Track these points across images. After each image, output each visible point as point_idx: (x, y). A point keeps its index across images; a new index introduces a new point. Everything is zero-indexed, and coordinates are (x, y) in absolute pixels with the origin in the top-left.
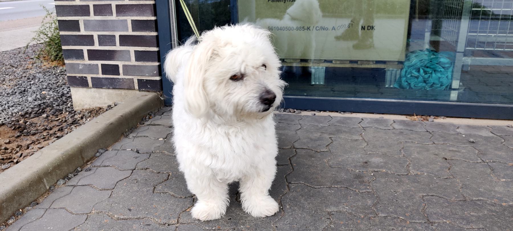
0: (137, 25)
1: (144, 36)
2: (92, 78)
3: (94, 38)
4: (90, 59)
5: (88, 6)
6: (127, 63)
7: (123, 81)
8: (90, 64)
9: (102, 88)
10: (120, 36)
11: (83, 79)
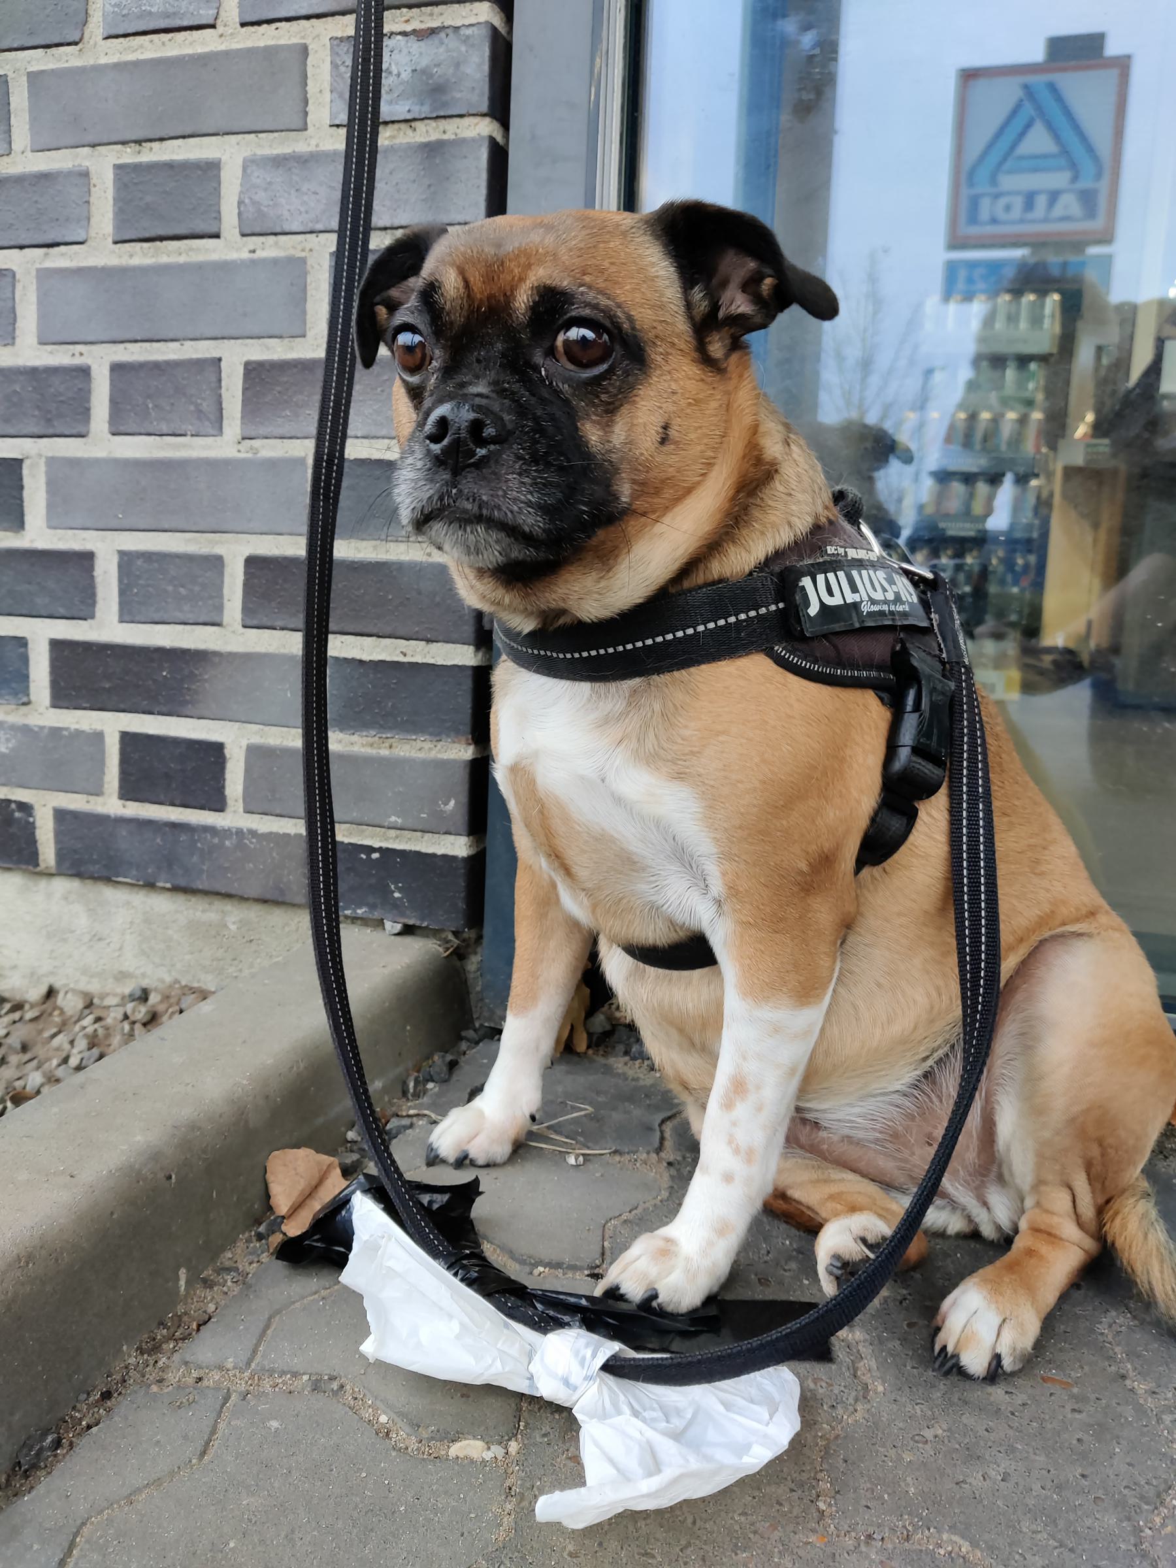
1: (400, 566)
2: (61, 815)
3: (98, 572)
4: (62, 697)
5: (84, 372)
7: (240, 846)
8: (56, 732)
9: (108, 880)
10: (252, 563)
11: (9, 821)
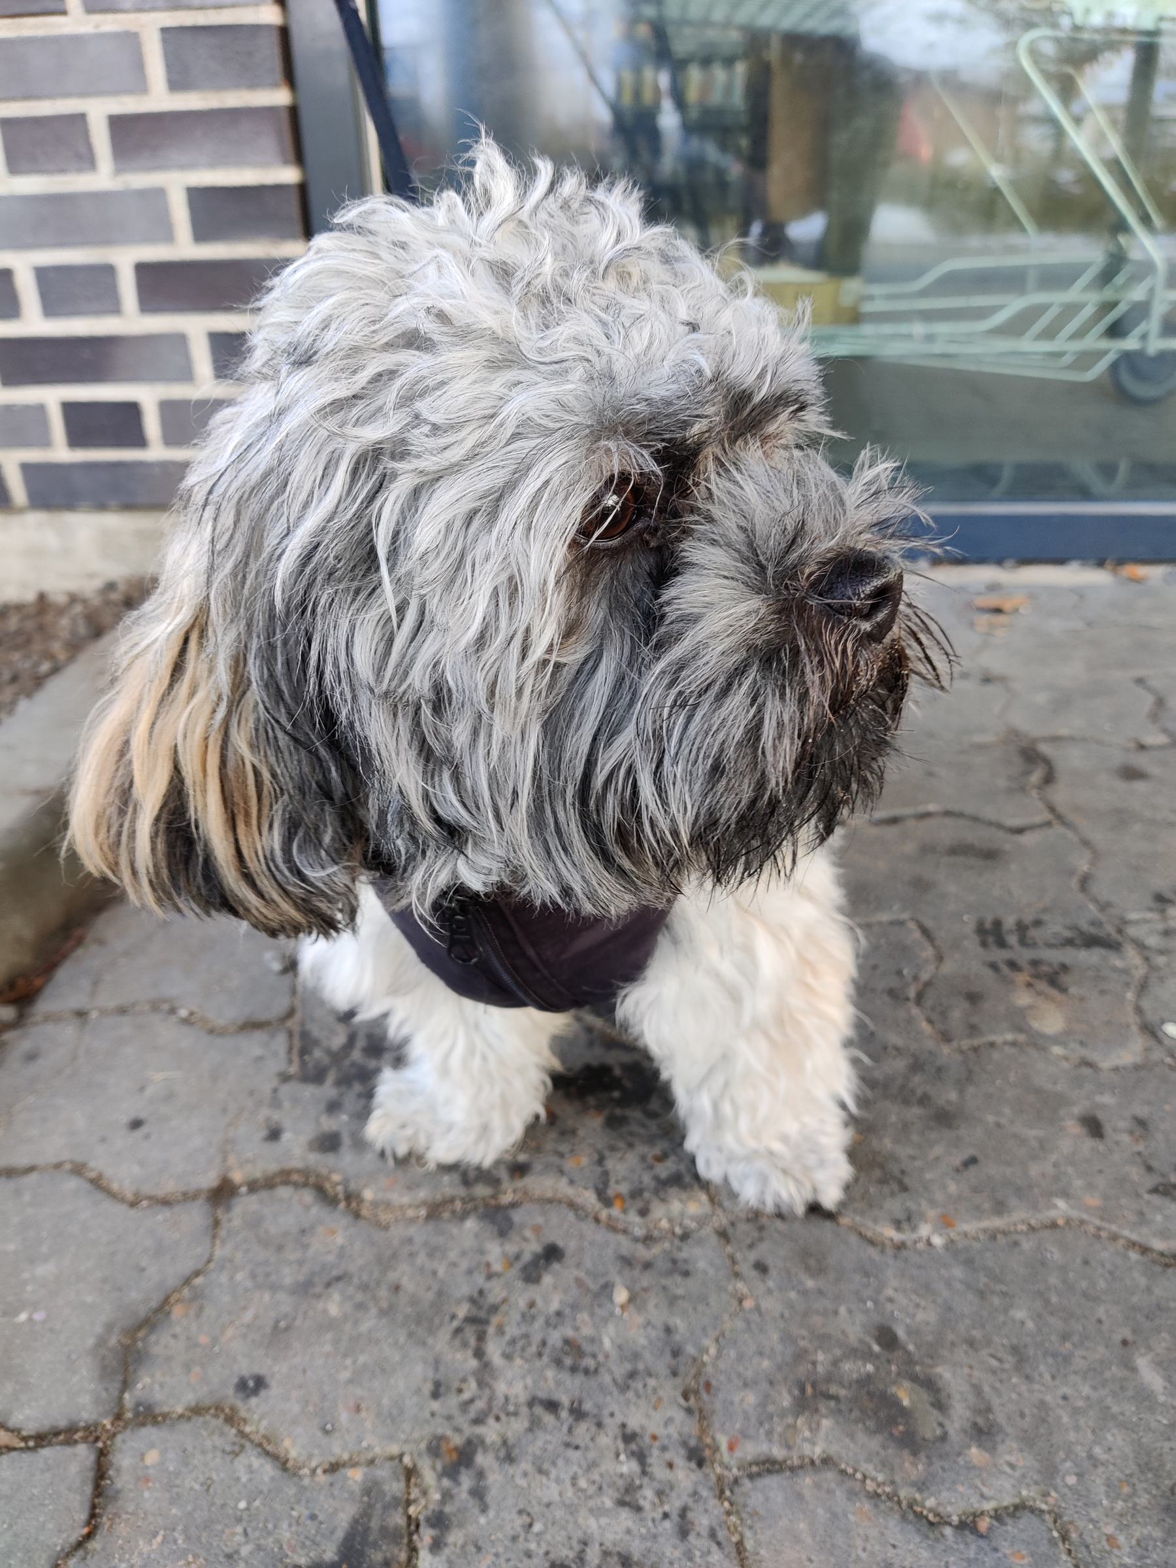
0: (216, 210)
6: (178, 391)
10: (144, 270)
